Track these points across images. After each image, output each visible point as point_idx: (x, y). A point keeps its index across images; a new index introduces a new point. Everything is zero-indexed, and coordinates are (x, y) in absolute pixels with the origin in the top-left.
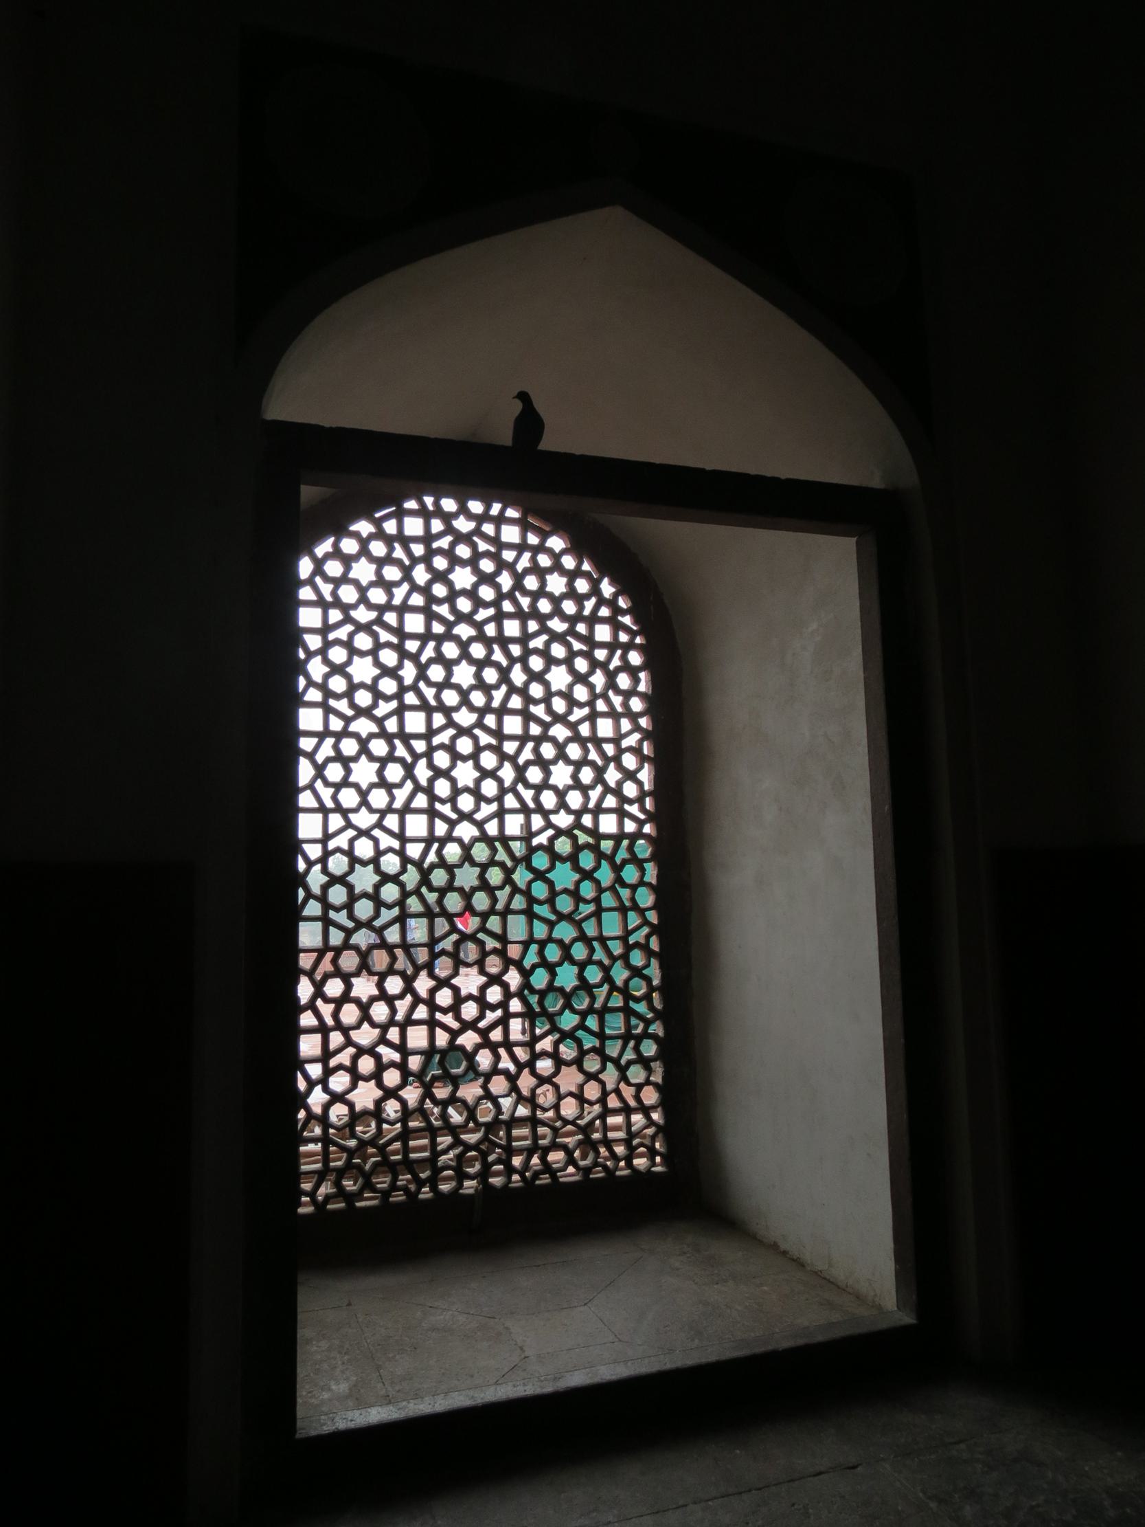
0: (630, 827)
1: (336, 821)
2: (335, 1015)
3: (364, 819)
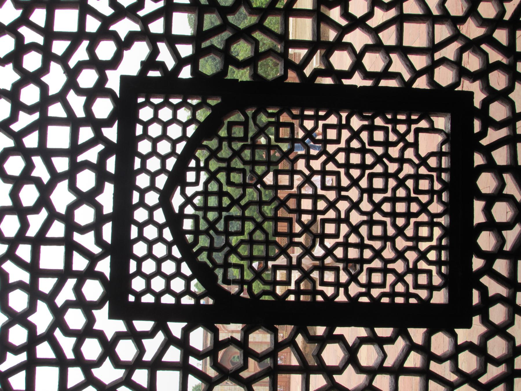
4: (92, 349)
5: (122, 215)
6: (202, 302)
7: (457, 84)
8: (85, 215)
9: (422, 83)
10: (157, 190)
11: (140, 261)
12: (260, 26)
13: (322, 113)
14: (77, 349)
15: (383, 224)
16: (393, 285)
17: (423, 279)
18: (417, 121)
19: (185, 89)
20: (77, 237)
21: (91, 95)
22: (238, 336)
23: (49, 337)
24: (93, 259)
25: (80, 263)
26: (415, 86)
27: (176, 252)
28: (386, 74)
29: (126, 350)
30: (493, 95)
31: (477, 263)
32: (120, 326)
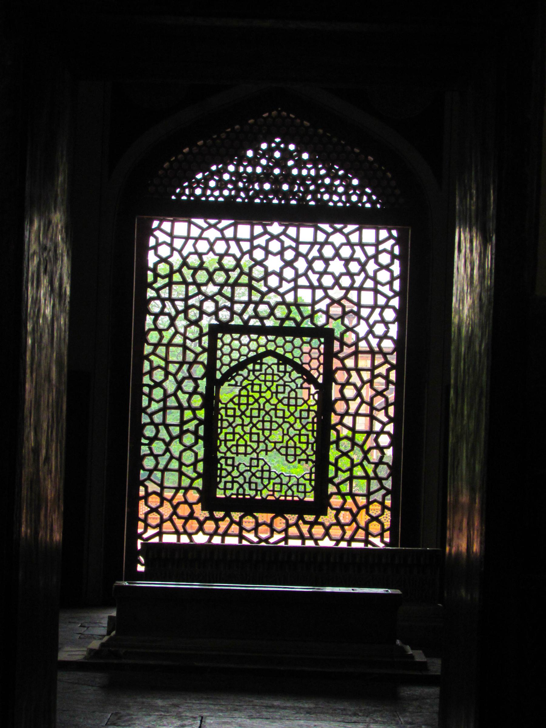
0: (381, 301)
1: (193, 289)
2: (189, 400)
3: (211, 289)
4: (193, 314)
5: (263, 331)
6: (218, 373)
7: (332, 509)
8: (263, 309)
9: (332, 489)
10: (276, 349)
11: (239, 339)
12: (363, 402)
13: (315, 433)
14: (193, 306)
15: (258, 466)
16: (226, 470)
17: (229, 485)
18: (310, 484)
19: (327, 364)
20: (252, 306)
22: (199, 390)
23: (200, 292)
24: (241, 315)
25: (238, 308)
26: (330, 486)
27: (243, 359)
28: (337, 469)
29: (193, 332)
30: (327, 530)
31: (236, 516)
32: (206, 330)
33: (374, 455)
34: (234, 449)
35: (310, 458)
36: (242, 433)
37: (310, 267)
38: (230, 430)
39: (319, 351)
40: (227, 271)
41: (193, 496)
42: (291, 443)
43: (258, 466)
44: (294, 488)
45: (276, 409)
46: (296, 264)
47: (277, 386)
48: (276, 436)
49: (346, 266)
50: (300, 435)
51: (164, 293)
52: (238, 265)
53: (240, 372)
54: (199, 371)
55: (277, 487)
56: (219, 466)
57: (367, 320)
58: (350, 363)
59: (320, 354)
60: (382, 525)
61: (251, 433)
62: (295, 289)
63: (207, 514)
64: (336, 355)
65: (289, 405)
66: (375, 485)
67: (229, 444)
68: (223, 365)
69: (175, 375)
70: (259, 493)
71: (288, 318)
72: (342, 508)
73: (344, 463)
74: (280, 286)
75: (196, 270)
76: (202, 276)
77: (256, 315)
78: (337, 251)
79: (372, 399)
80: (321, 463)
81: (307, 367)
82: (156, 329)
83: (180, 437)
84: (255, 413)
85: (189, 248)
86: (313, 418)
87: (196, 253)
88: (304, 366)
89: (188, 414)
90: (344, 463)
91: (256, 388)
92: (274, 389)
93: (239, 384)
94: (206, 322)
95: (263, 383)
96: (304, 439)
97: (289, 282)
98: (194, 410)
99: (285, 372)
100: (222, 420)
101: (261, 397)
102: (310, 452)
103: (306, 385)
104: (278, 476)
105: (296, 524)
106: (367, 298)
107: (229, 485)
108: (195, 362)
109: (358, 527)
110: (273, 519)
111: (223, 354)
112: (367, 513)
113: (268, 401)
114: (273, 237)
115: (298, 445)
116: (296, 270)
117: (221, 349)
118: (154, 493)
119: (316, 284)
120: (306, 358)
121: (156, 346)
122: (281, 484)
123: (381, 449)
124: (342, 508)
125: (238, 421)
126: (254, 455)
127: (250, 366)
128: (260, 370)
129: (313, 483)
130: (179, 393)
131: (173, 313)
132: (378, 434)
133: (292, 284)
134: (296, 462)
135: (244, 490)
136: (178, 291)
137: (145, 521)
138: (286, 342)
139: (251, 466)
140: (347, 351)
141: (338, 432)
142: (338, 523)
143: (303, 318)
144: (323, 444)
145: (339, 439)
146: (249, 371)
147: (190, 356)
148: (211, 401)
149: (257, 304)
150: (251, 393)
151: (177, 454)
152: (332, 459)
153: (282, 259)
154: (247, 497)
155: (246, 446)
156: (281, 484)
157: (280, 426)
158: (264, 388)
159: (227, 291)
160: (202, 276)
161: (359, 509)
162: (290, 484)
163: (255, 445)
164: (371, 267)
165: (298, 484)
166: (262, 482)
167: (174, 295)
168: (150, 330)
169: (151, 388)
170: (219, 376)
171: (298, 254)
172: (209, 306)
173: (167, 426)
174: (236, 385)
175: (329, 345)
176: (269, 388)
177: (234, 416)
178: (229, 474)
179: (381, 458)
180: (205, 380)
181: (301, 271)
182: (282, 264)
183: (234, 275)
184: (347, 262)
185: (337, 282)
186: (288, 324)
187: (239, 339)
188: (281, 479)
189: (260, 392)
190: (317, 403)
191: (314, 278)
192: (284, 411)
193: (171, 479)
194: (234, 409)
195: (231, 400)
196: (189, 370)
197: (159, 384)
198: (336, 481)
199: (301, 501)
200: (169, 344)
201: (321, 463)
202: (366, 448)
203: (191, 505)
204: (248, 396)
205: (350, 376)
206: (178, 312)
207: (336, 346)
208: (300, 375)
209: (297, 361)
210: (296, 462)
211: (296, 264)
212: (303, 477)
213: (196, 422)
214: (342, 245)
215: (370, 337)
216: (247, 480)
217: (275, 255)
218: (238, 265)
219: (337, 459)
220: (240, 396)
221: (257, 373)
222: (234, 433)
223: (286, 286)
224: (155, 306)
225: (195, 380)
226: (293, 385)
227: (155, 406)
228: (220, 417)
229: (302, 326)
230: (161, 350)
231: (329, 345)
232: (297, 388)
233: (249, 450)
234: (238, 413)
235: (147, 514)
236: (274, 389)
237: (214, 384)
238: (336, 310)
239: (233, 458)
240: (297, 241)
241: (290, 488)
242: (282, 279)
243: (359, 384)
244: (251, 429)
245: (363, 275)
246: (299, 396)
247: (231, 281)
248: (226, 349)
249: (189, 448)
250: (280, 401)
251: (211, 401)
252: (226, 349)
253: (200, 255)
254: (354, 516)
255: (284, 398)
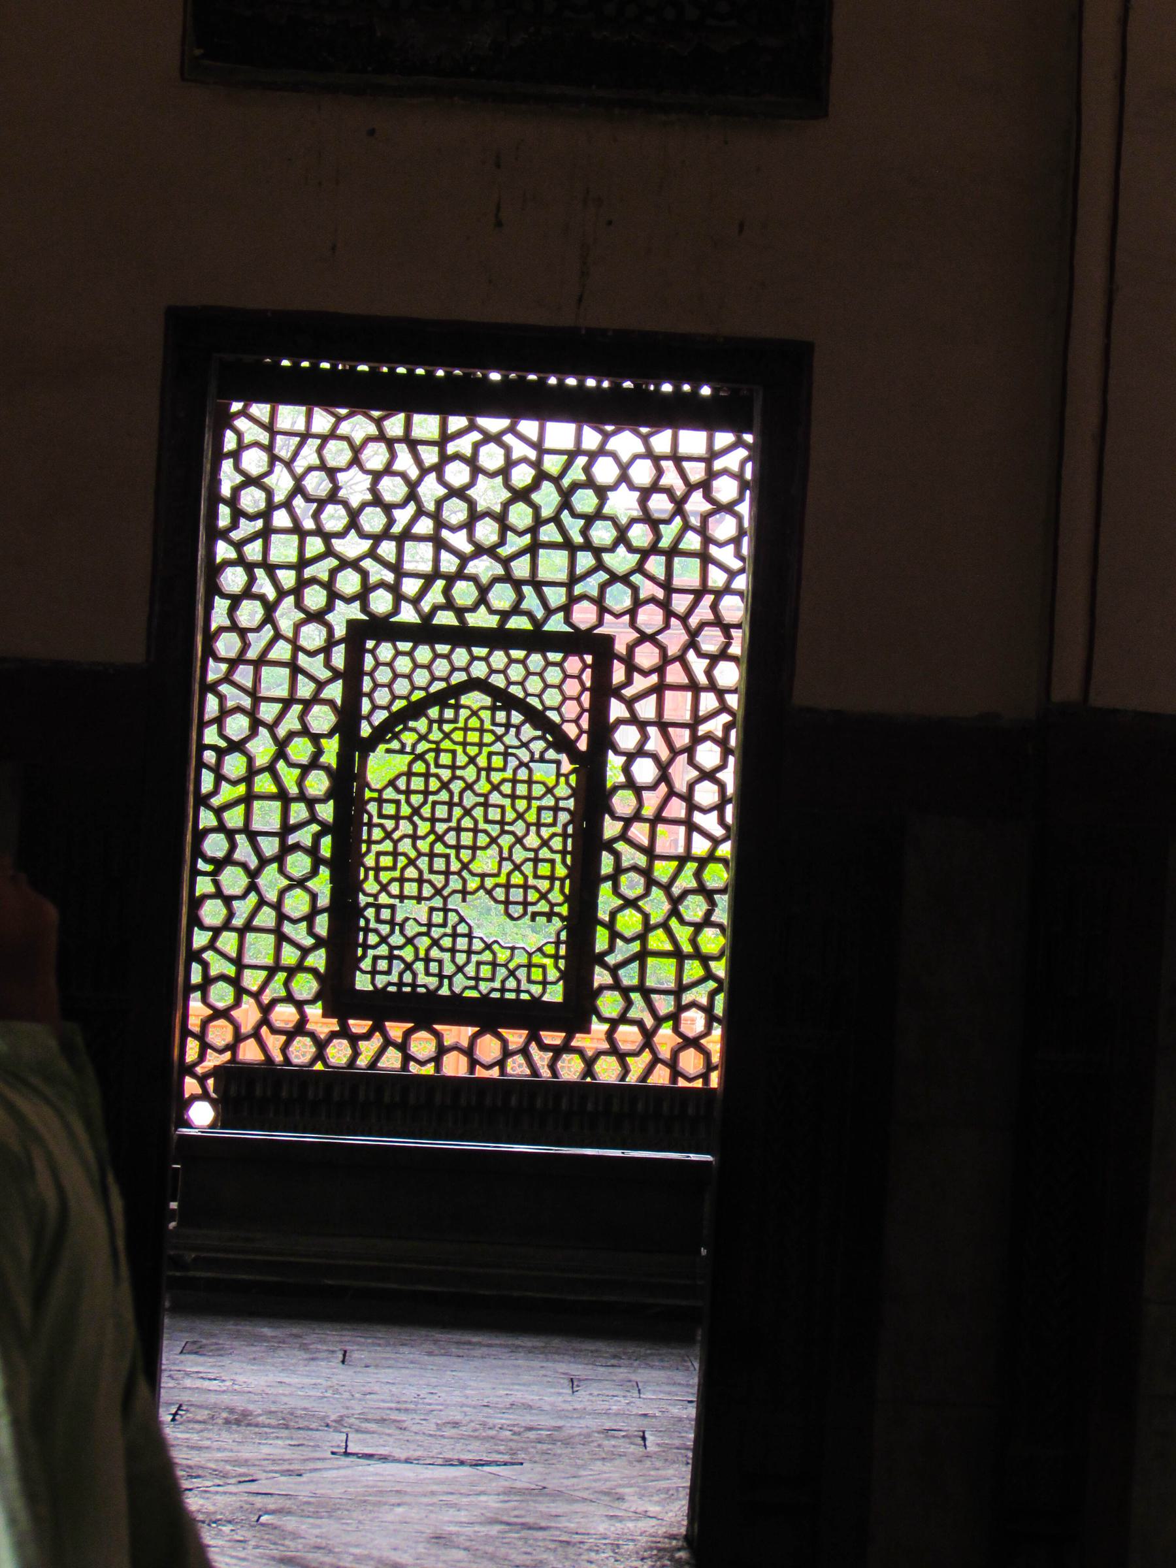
1: (315, 546)
3: (352, 546)
5: (463, 636)
7: (602, 1019)
8: (464, 593)
9: (601, 977)
10: (489, 676)
11: (410, 654)
12: (672, 793)
13: (569, 858)
14: (314, 581)
15: (444, 925)
16: (376, 931)
18: (556, 967)
19: (598, 711)
20: (440, 584)
21: (599, 602)
22: (323, 759)
23: (329, 552)
24: (416, 601)
25: (411, 587)
26: (598, 969)
27: (418, 695)
28: (614, 935)
29: (313, 636)
31: (396, 1030)
32: (340, 631)
33: (694, 908)
34: (395, 888)
35: (557, 909)
36: (413, 854)
37: (566, 504)
38: (388, 846)
39: (582, 683)
40: (388, 509)
41: (305, 986)
42: (517, 879)
43: (444, 925)
44: (522, 973)
45: (486, 805)
46: (535, 497)
47: (490, 755)
48: (486, 861)
49: (643, 502)
50: (536, 861)
51: (253, 551)
52: (412, 495)
53: (411, 724)
54: (322, 719)
55: (486, 971)
56: (362, 923)
57: (684, 619)
58: (646, 709)
59: (584, 689)
60: (707, 1055)
61: (432, 855)
62: (533, 549)
63: (333, 1025)
64: (617, 693)
65: (513, 797)
66: (694, 970)
67: (385, 877)
68: (375, 707)
69: (272, 728)
70: (446, 981)
71: (516, 610)
72: (623, 1019)
73: (629, 922)
74: (502, 542)
75: (322, 504)
76: (334, 518)
77: (449, 605)
78: (624, 468)
79: (691, 787)
80: (581, 920)
81: (554, 716)
82: (234, 627)
83: (279, 859)
84: (442, 812)
85: (308, 457)
86: (565, 826)
87: (323, 467)
88: (548, 713)
89: (299, 812)
90: (629, 922)
91: (445, 759)
92: (482, 761)
93: (408, 749)
94: (343, 615)
95: (459, 749)
96: (544, 869)
97: (521, 534)
98: (311, 803)
99: (508, 725)
100: (371, 825)
101: (454, 777)
102: (556, 896)
103: (551, 754)
104: (488, 947)
105: (524, 1051)
106: (687, 573)
107: (383, 965)
108: (316, 699)
109: (656, 1060)
110: (474, 1038)
111: (376, 685)
112: (676, 1030)
113: (469, 787)
114: (488, 438)
115: (531, 881)
116: (536, 509)
117: (371, 674)
118: (223, 977)
119: (578, 539)
120: (552, 698)
121: (234, 663)
122: (494, 964)
123: (709, 895)
124: (623, 1019)
125: (405, 827)
126: (438, 902)
127: (434, 712)
128: (455, 720)
129: (562, 964)
130: (281, 765)
131: (271, 594)
132: (703, 862)
133: (527, 539)
134: (528, 917)
135: (415, 975)
136: (284, 549)
137: (201, 1037)
138: (512, 661)
139: (430, 925)
140: (641, 683)
141: (617, 855)
142: (614, 1050)
143: (550, 612)
144: (584, 882)
145: (619, 870)
146: (431, 722)
147: (305, 689)
148: (347, 784)
149: (451, 580)
150: (433, 770)
151: (272, 896)
152: (603, 915)
153: (507, 485)
154: (422, 990)
155: (420, 881)
156: (494, 964)
157: (494, 840)
158: (462, 760)
159: (387, 549)
160: (334, 518)
161: (659, 1020)
162: (512, 966)
163: (439, 880)
164: (697, 504)
165: (529, 966)
166: (453, 960)
167: (275, 557)
168: (222, 629)
169: (221, 753)
170: (365, 731)
171: (541, 476)
172: (349, 582)
173: (252, 836)
174: (402, 751)
175: (602, 671)
176: (472, 760)
177: (397, 817)
178: (384, 940)
179: (709, 913)
180: (337, 737)
181: (546, 513)
182: (507, 495)
183: (402, 516)
184: (646, 494)
185: (622, 538)
186: (518, 623)
187: (410, 654)
188: (494, 954)
189: (453, 767)
190: (575, 793)
191: (575, 528)
192: (503, 808)
193: (260, 948)
194: (397, 803)
195: (392, 783)
196: (302, 717)
197: (236, 747)
198: (611, 960)
199: (536, 1001)
200: (261, 661)
201: (581, 920)
202: (676, 890)
203: (300, 1005)
204: (427, 776)
205: (645, 738)
206: (282, 594)
207: (618, 674)
208: (539, 733)
209: (534, 702)
210: (528, 917)
211: (535, 497)
212: (540, 950)
213: (315, 828)
214: (636, 457)
215: (691, 655)
216: (422, 954)
217: (492, 475)
218: (412, 495)
219: (613, 914)
220: (409, 774)
221: (447, 727)
222: (395, 854)
223: (515, 543)
224: (234, 579)
225: (315, 739)
226: (524, 755)
227: (228, 793)
228: (366, 818)
229: (546, 628)
230: (244, 675)
231: (602, 671)
232: (532, 760)
233: (427, 891)
234: (406, 810)
235: (205, 1023)
236: (482, 761)
237: (355, 748)
238: (619, 598)
239: (392, 907)
240: (538, 446)
241: (512, 973)
242: (505, 527)
243: (664, 754)
244: (432, 845)
245: (678, 521)
246: (537, 776)
247: (396, 529)
248: (384, 675)
249: (301, 883)
250: (496, 788)
251: (347, 784)
252: (384, 675)
253: (332, 473)
254: (648, 1036)
255: (504, 781)
